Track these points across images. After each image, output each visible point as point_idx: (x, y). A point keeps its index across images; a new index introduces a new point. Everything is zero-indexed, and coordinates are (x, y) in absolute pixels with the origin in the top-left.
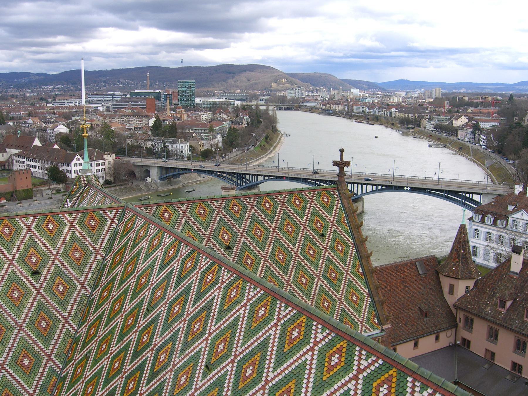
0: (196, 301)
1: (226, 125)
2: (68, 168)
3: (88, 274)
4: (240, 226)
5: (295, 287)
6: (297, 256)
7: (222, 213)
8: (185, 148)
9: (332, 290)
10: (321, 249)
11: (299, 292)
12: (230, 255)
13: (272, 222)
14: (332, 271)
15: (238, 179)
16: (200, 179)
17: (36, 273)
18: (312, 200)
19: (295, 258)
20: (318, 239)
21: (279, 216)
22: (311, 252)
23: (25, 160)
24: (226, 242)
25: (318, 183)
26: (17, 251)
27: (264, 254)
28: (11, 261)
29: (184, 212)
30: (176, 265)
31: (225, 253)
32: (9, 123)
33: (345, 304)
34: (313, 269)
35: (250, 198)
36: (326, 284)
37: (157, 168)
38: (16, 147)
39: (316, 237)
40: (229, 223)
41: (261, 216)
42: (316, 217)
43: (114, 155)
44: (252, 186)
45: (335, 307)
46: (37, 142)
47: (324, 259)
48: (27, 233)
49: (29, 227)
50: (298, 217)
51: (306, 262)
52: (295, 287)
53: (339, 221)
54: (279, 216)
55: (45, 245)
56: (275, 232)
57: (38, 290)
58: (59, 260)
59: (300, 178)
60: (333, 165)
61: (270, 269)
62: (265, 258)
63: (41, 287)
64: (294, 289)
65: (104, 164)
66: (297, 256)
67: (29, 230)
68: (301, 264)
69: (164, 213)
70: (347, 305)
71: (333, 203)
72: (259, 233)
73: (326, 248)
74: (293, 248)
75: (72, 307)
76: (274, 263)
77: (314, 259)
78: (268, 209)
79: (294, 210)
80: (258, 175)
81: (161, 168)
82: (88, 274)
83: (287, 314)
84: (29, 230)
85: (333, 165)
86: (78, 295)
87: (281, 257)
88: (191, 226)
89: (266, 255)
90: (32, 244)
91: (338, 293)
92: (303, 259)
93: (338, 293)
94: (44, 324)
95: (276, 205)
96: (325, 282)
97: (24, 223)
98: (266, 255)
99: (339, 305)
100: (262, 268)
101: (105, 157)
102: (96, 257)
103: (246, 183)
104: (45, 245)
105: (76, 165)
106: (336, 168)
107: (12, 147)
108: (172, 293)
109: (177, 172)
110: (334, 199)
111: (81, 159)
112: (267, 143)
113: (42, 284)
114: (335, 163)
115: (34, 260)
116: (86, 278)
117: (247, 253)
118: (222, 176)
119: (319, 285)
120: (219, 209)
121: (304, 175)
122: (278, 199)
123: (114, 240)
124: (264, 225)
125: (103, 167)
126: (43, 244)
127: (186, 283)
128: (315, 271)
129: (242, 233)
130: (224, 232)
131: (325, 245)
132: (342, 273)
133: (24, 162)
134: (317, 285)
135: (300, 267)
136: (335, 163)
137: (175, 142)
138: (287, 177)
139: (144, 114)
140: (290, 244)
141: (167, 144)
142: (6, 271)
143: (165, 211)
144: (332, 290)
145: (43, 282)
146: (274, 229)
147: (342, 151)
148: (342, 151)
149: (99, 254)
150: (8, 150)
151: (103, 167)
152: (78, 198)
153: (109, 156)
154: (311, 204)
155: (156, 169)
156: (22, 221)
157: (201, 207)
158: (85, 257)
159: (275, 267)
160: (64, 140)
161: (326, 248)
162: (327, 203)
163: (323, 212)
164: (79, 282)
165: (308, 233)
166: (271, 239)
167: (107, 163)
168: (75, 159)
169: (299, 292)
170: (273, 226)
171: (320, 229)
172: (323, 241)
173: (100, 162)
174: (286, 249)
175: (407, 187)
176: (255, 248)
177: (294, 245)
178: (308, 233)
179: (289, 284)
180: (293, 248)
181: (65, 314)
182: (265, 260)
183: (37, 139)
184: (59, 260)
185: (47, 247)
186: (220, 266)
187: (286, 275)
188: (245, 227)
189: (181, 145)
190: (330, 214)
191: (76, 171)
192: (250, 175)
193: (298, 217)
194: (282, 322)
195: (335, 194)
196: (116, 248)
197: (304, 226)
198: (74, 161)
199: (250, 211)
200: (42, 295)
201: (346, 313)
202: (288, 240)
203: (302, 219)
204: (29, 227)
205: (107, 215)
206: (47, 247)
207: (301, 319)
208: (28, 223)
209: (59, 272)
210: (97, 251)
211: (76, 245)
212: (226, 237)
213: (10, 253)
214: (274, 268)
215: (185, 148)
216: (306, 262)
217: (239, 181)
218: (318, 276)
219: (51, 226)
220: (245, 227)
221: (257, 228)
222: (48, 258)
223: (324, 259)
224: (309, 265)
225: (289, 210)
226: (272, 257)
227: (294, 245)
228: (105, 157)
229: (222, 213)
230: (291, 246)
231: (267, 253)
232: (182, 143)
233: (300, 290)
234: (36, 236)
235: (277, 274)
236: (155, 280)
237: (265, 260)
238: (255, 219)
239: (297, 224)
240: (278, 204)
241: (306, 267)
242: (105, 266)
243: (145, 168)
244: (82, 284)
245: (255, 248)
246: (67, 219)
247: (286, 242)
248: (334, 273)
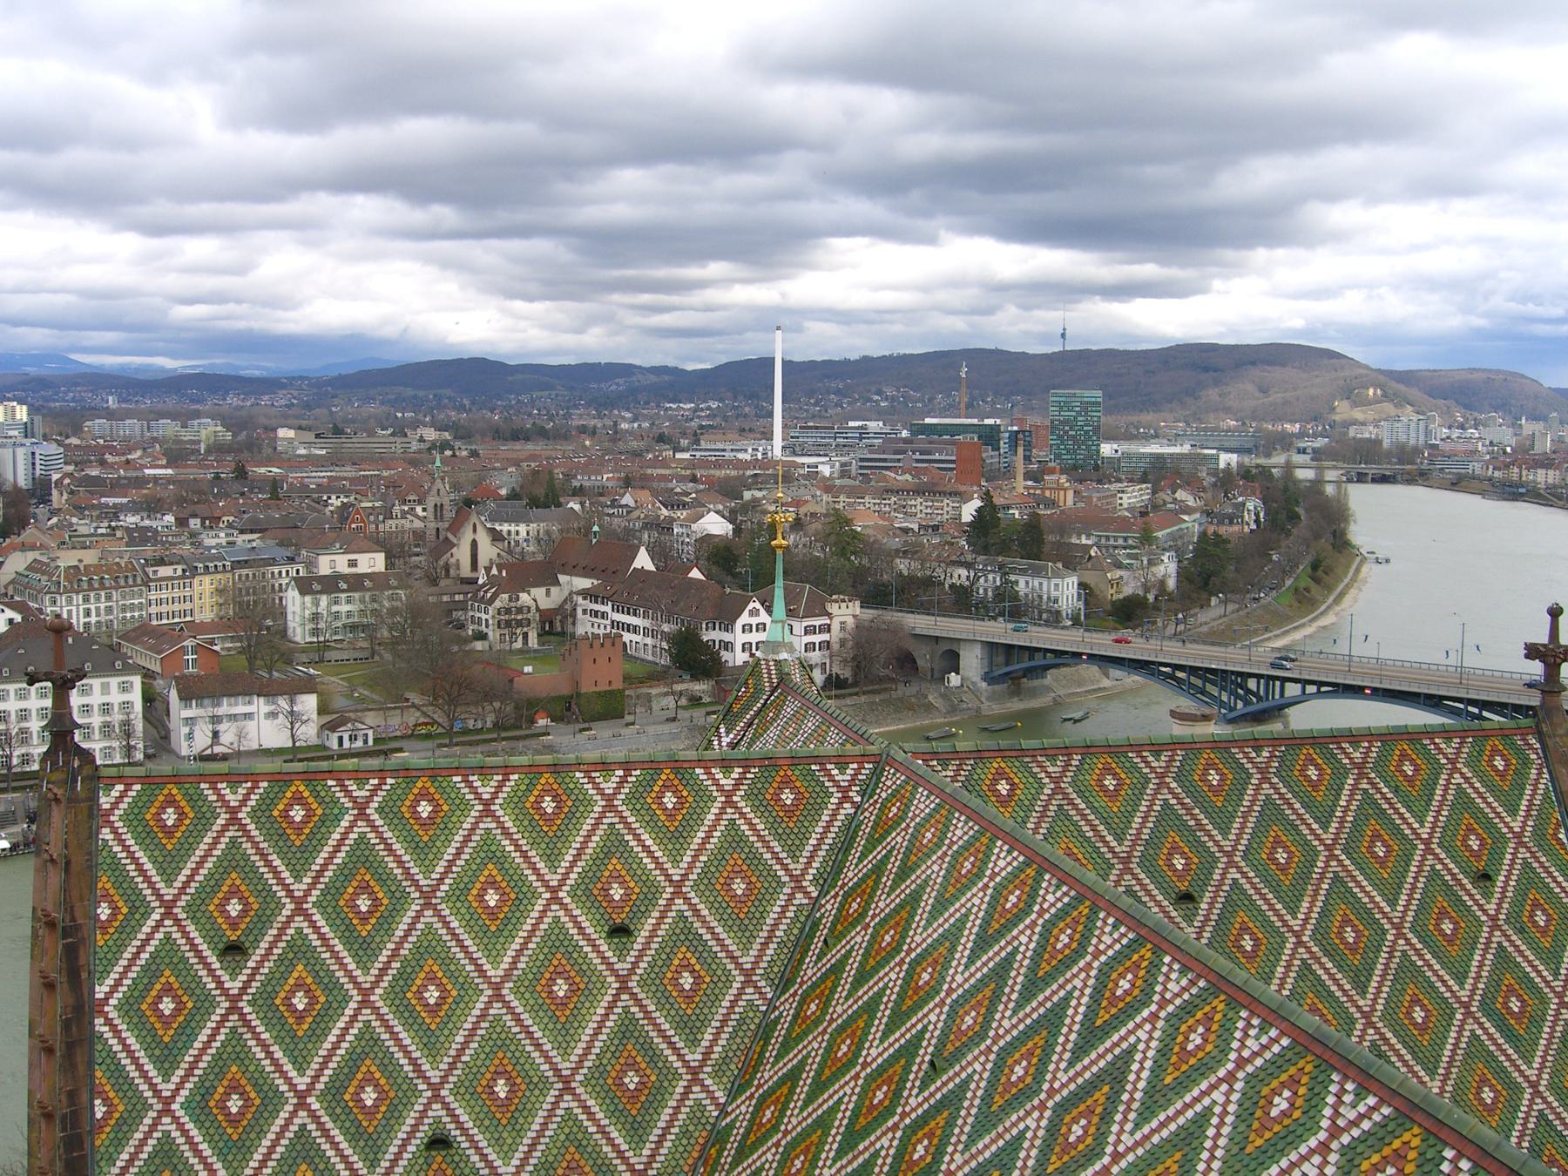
0: (1079, 1052)
1: (1192, 524)
2: (727, 637)
3: (765, 945)
4: (1225, 832)
5: (1389, 1035)
6: (1400, 935)
7: (1171, 791)
8: (1065, 590)
9: (1510, 1051)
10: (1477, 919)
11: (1403, 1051)
12: (1189, 919)
13: (1325, 826)
14: (1511, 991)
15: (1223, 688)
16: (1106, 683)
17: (620, 932)
18: (1453, 762)
19: (1394, 942)
20: (1469, 886)
21: (1346, 809)
22: (1447, 927)
23: (608, 608)
24: (1180, 878)
25: (1476, 711)
26: (573, 864)
27: (1296, 924)
28: (554, 891)
29: (1057, 781)
30: (1024, 939)
31: (1174, 914)
32: (571, 505)
33: (1551, 1099)
34: (1451, 983)
35: (1258, 749)
36: (1492, 1030)
37: (979, 646)
38: (586, 572)
39: (1465, 881)
40: (1192, 823)
41: (1290, 806)
42: (1467, 819)
43: (858, 603)
44: (1264, 711)
45: (1516, 1108)
46: (643, 561)
47: (1485, 951)
48: (602, 815)
49: (609, 799)
50: (1407, 815)
51: (1428, 956)
52: (1389, 1035)
53: (1539, 834)
54: (1346, 809)
55: (650, 853)
56: (1332, 857)
57: (623, 982)
58: (687, 900)
59: (1417, 695)
60: (1527, 656)
61: (1313, 972)
62: (1297, 935)
63: (632, 971)
64: (1386, 1040)
65: (828, 629)
66: (1400, 935)
67: (610, 807)
68: (1413, 963)
69: (995, 781)
70: (1556, 1104)
71: (1521, 774)
72: (1281, 856)
73: (1494, 919)
74: (1387, 909)
75: (715, 1039)
76: (1327, 953)
77: (1454, 950)
78: (1315, 786)
79: (1396, 791)
80: (1284, 680)
81: (992, 647)
82: (765, 945)
83: (1361, 1117)
84: (610, 807)
85: (1527, 656)
86: (734, 1003)
87: (1350, 936)
88: (1075, 824)
89: (1303, 926)
90: (614, 846)
91: (1529, 1064)
92: (1419, 946)
93: (1529, 1064)
94: (632, 1080)
95: (1340, 773)
96: (1487, 1025)
97: (597, 787)
98: (1303, 926)
99: (1532, 1101)
100: (1288, 966)
101: (833, 608)
102: (791, 897)
103: (1247, 703)
104: (650, 853)
105: (747, 628)
106: (1536, 668)
107: (574, 570)
108: (1007, 1023)
109: (1039, 661)
110: (1526, 763)
111: (762, 611)
112: (1317, 581)
113: (635, 965)
114: (1532, 652)
115: (617, 893)
116: (759, 957)
117: (1242, 916)
118: (1173, 677)
119: (1467, 1033)
120: (1161, 776)
121: (1429, 683)
122: (1348, 755)
123: (847, 851)
124: (1299, 833)
125: (826, 637)
126: (646, 848)
127: (1051, 994)
128: (1456, 988)
129: (1229, 855)
130: (1175, 849)
131: (1491, 908)
132: (1544, 1001)
133: (604, 615)
134: (1460, 1033)
135: (1407, 972)
136: (1532, 652)
137: (1037, 572)
138: (1375, 690)
139: (948, 489)
140: (1378, 899)
141: (1012, 578)
142: (540, 919)
143: (1000, 775)
144: (1510, 1051)
145: (639, 958)
146: (1329, 848)
147: (1555, 613)
148: (1555, 613)
149: (801, 888)
150: (562, 578)
151: (826, 637)
152: (750, 724)
153: (843, 605)
154: (1450, 776)
155: (977, 651)
156: (592, 780)
157: (1107, 770)
158: (758, 898)
159: (1329, 965)
160: (719, 556)
161: (1494, 919)
162: (1502, 775)
163: (1489, 804)
164: (739, 966)
165: (1439, 867)
166: (1321, 880)
167: (835, 627)
168: (746, 612)
169: (1403, 1051)
170: (1328, 838)
171: (1477, 856)
172: (1487, 895)
173: (817, 622)
174: (1365, 915)
176: (1268, 902)
177: (1393, 903)
178: (1439, 867)
179: (1370, 1024)
180: (1387, 909)
181: (694, 1057)
182: (1300, 943)
183: (643, 549)
184: (687, 900)
185: (655, 859)
186: (1158, 951)
187: (1363, 993)
188: (1239, 837)
189: (1054, 581)
190: (1513, 812)
191: (746, 647)
192: (1258, 676)
193: (1407, 815)
194: (1345, 1139)
195: (1531, 747)
196: (851, 875)
197: (1427, 843)
198: (745, 618)
199: (1258, 789)
200: (633, 996)
201: (1553, 1128)
202: (1374, 885)
203: (1422, 823)
204: (609, 799)
205: (831, 778)
206: (655, 859)
207: (1407, 1136)
208: (609, 787)
209: (684, 934)
210: (797, 880)
211: (738, 857)
212: (1179, 863)
213: (553, 868)
214: (1326, 969)
215: (1065, 590)
216: (1428, 956)
217: (1225, 698)
218: (1466, 1006)
219: (669, 800)
220: (1239, 837)
221: (1277, 842)
222: (658, 891)
223: (1485, 951)
224: (1437, 967)
225: (1379, 790)
226: (1320, 934)
227: (1393, 903)
228: (833, 608)
229: (1171, 791)
230: (1383, 904)
231: (1306, 921)
232: (1057, 575)
233: (1404, 1043)
234: (627, 825)
235: (1334, 988)
236: (960, 978)
237: (1300, 943)
238: (1271, 813)
239: (1405, 837)
240: (1347, 771)
241: (1429, 974)
242: (815, 925)
243: (945, 647)
244: (748, 974)
245: (1268, 902)
246: (716, 783)
247: (1366, 891)
248: (1519, 997)
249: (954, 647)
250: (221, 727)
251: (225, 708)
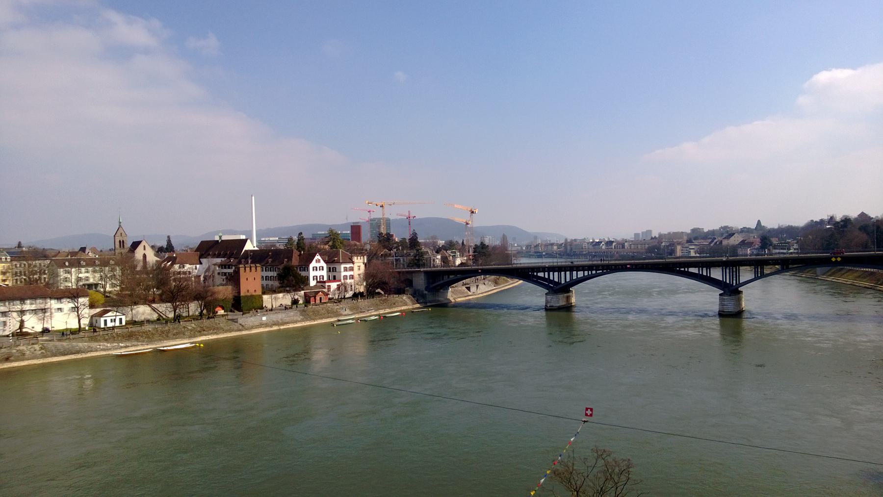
65: (352, 269)
101: (355, 259)
105: (315, 269)
109: (446, 279)
125: (351, 273)
151: (351, 273)
155: (422, 276)
167: (356, 268)
173: (348, 266)
175: (836, 258)
191: (315, 278)
198: (313, 264)
249: (409, 277)
250: (24, 318)
251: (28, 305)
